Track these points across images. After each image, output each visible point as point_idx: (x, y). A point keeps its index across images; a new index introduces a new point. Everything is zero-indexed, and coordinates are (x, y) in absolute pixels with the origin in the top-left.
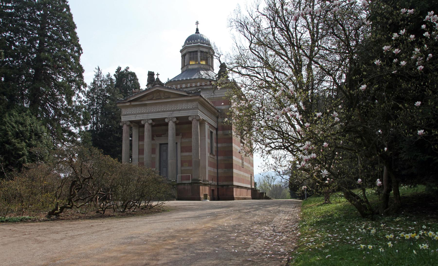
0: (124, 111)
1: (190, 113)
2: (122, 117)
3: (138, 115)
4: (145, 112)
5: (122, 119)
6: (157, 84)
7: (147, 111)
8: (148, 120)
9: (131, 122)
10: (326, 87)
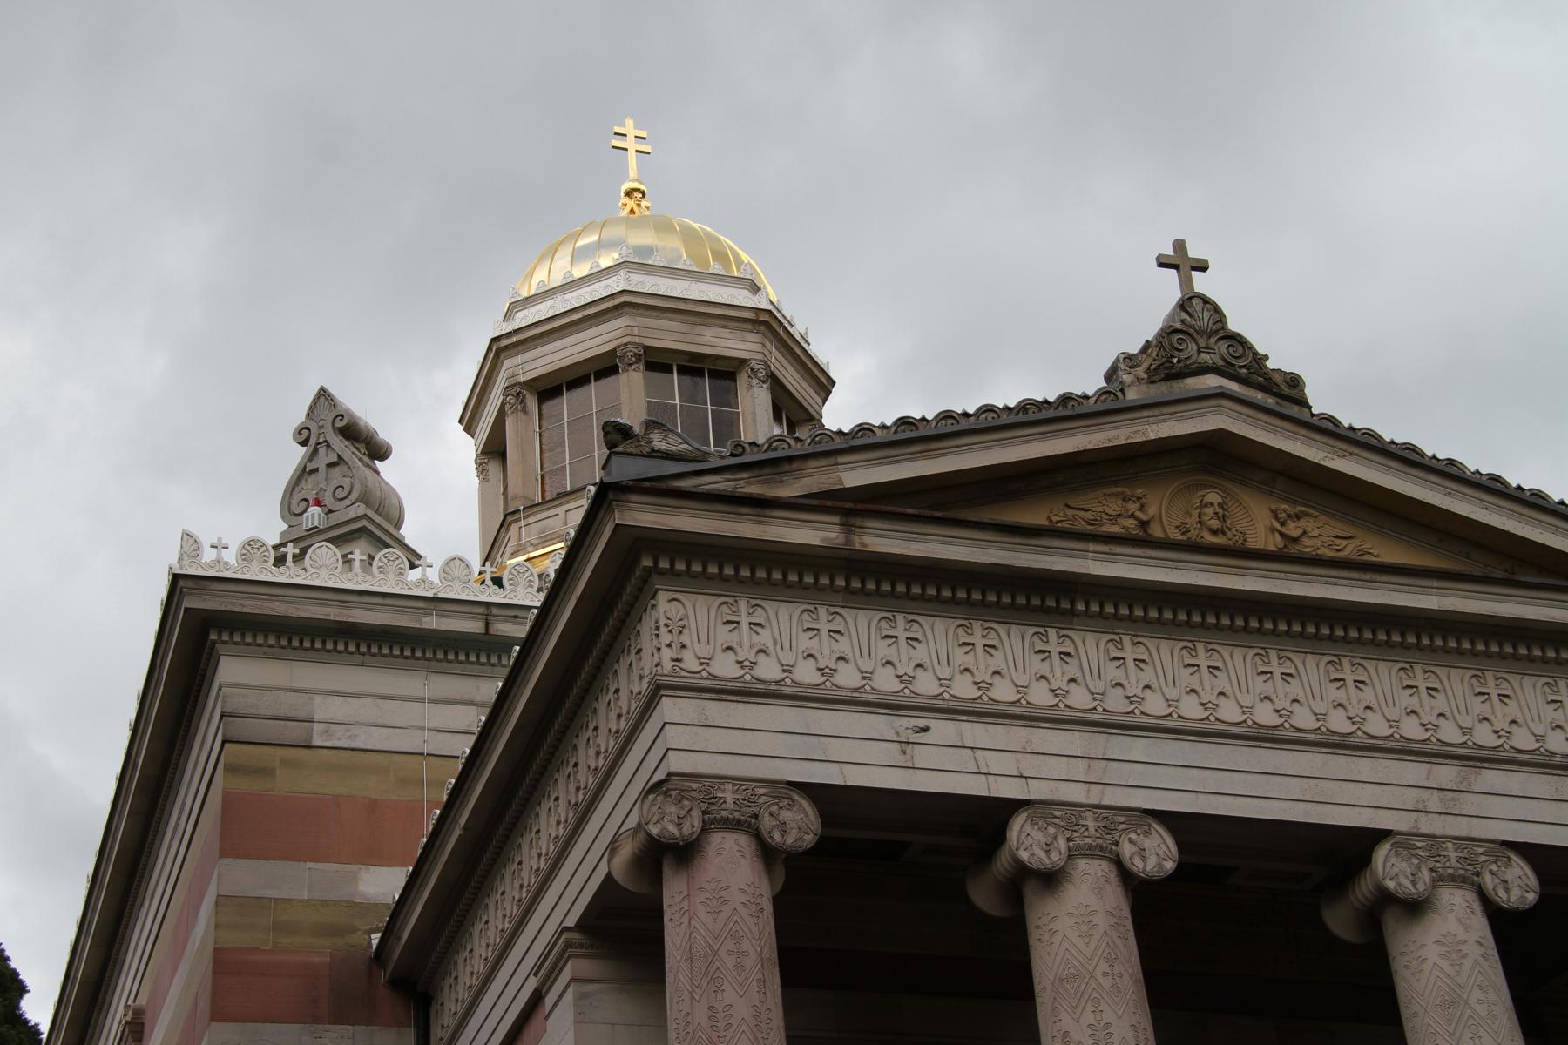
3: (943, 729)
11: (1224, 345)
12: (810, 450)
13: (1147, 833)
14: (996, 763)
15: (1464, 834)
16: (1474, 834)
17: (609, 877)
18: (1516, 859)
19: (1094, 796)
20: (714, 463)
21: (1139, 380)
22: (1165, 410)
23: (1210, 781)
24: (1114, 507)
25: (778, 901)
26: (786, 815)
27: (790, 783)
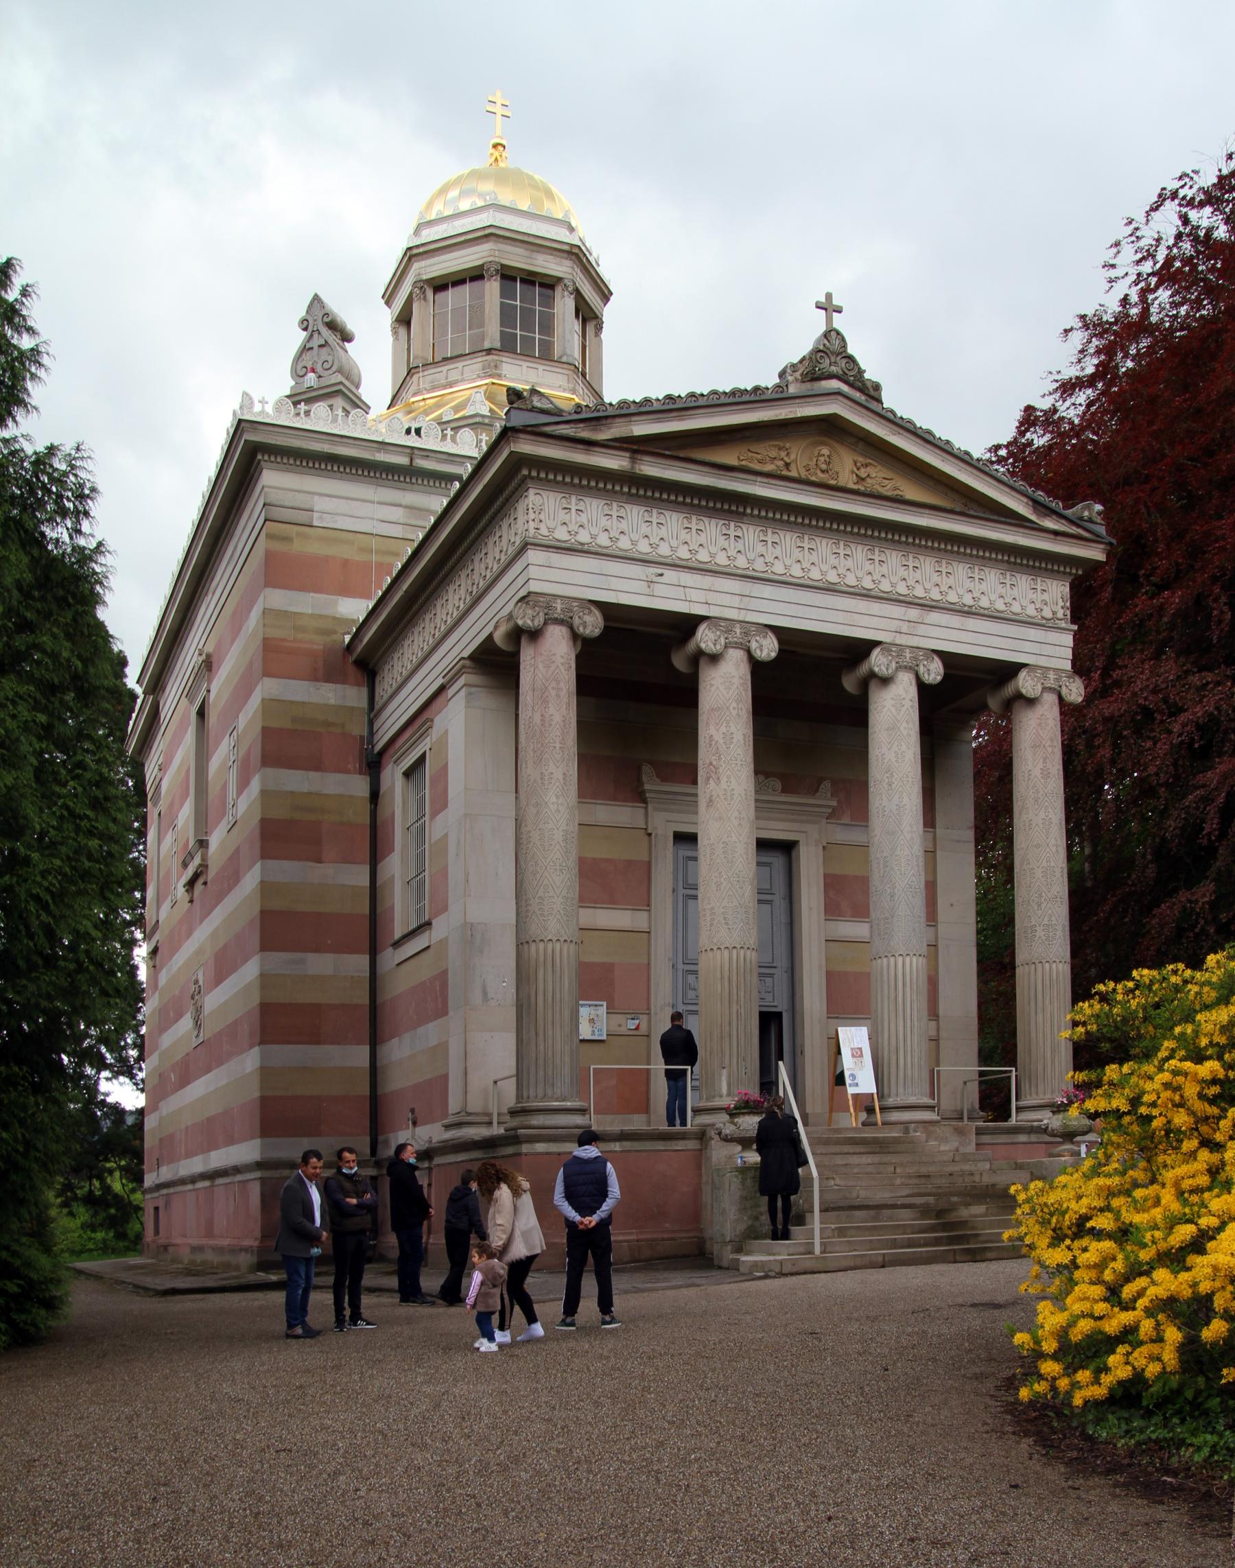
1: (1028, 647)
3: (670, 575)
6: (831, 376)
11: (844, 361)
12: (618, 412)
13: (765, 637)
14: (695, 595)
15: (915, 645)
16: (920, 645)
17: (490, 637)
18: (936, 658)
19: (742, 616)
21: (796, 379)
22: (808, 400)
23: (800, 611)
24: (773, 453)
25: (578, 657)
26: (587, 618)
27: (591, 601)
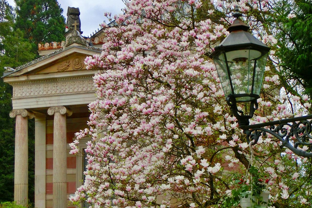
0: (17, 92)
2: (13, 102)
3: (42, 99)
4: (53, 92)
5: (13, 105)
6: (74, 43)
7: (58, 92)
8: (59, 107)
9: (30, 111)
10: (194, 135)
12: (21, 69)
20: (15, 71)
24: (66, 64)
27: (25, 109)
